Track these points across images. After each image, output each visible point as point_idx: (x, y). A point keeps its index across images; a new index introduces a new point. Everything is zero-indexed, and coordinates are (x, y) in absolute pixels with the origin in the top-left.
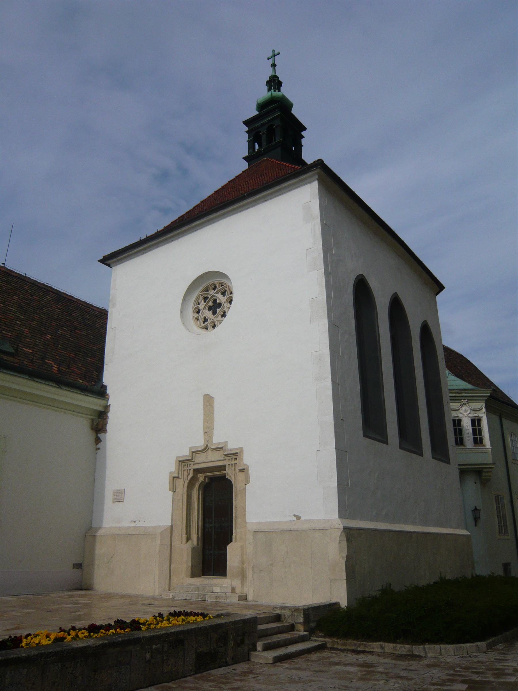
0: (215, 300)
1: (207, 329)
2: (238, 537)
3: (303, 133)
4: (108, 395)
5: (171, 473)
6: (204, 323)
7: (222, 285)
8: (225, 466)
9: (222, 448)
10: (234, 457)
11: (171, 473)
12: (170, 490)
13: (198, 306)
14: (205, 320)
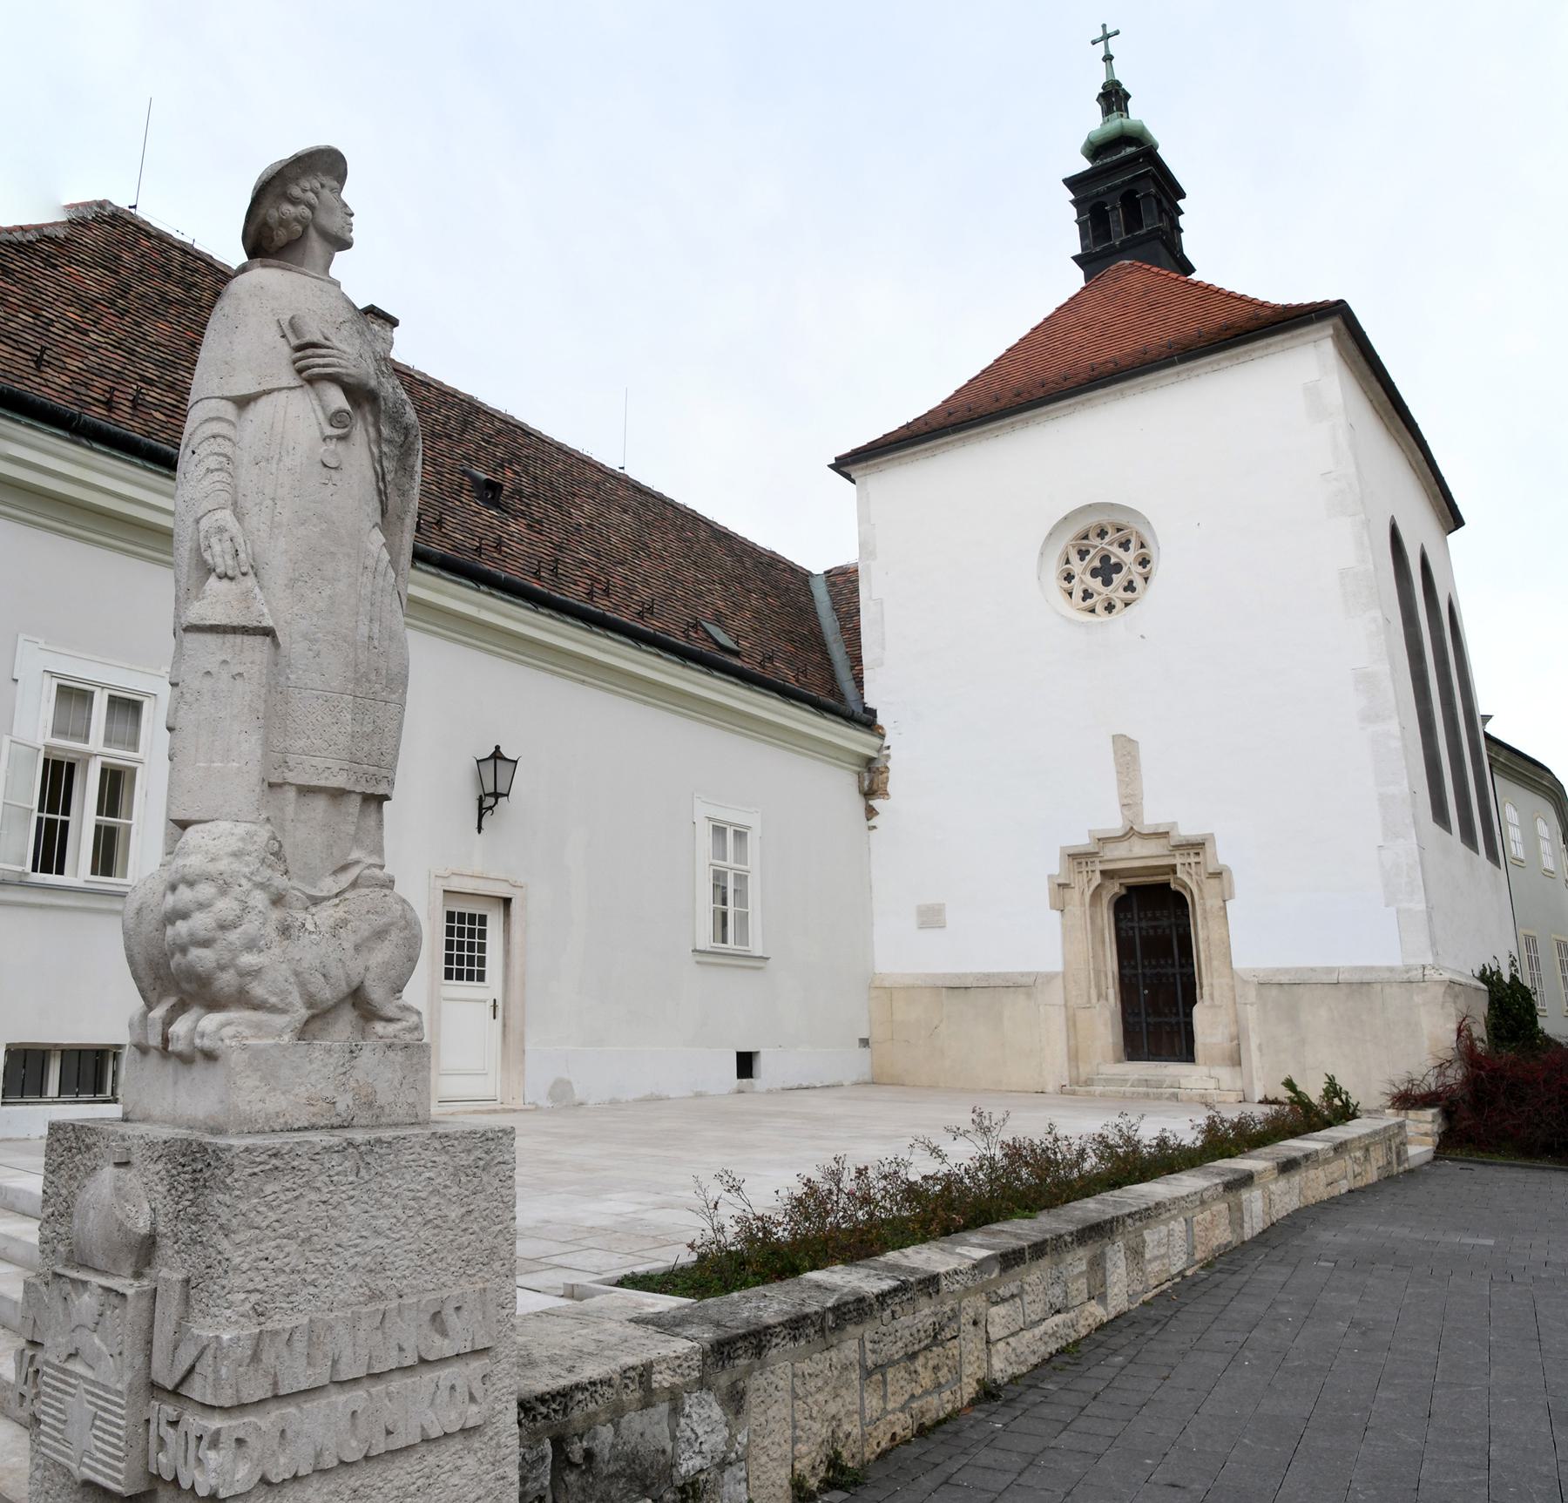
0: (1105, 559)
1: (1093, 611)
2: (1216, 994)
3: (1181, 203)
4: (881, 728)
5: (1050, 877)
6: (1084, 599)
7: (1119, 530)
8: (1175, 865)
9: (1168, 833)
10: (1192, 852)
11: (1050, 877)
12: (1052, 907)
13: (1068, 566)
14: (1087, 595)
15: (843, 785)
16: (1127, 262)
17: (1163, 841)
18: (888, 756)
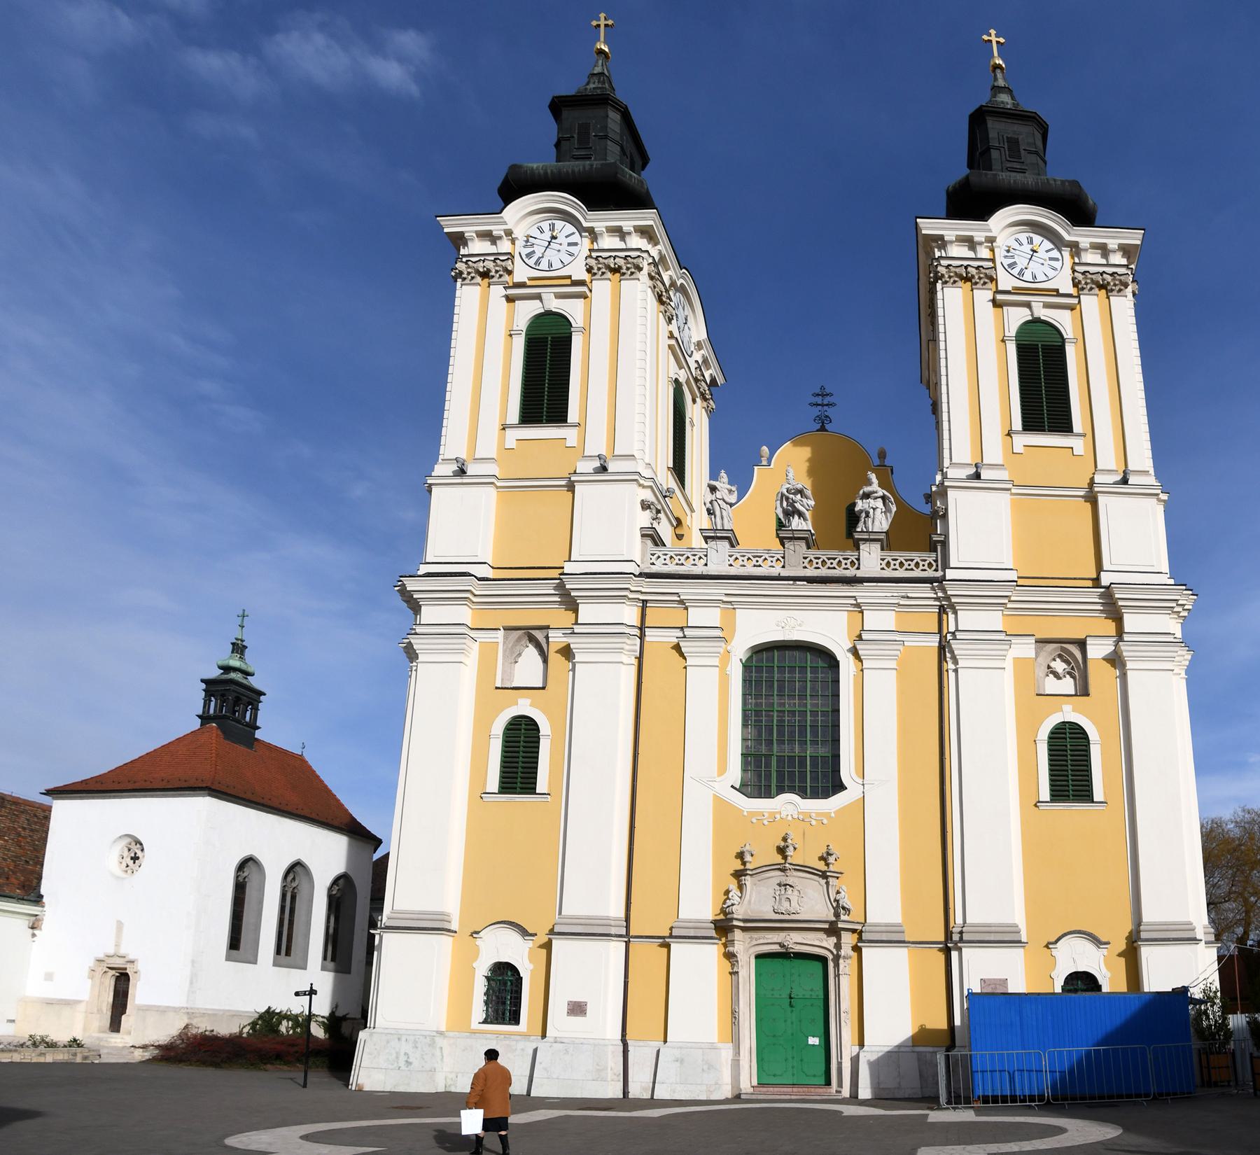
4: (44, 903)
15: (23, 923)
16: (214, 725)
17: (122, 959)
18: (44, 915)
